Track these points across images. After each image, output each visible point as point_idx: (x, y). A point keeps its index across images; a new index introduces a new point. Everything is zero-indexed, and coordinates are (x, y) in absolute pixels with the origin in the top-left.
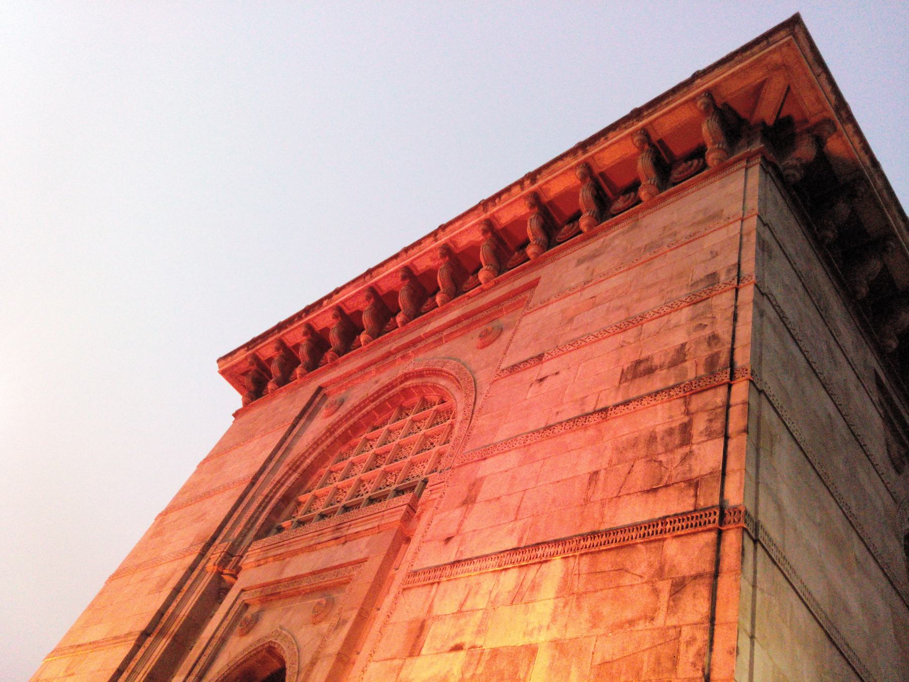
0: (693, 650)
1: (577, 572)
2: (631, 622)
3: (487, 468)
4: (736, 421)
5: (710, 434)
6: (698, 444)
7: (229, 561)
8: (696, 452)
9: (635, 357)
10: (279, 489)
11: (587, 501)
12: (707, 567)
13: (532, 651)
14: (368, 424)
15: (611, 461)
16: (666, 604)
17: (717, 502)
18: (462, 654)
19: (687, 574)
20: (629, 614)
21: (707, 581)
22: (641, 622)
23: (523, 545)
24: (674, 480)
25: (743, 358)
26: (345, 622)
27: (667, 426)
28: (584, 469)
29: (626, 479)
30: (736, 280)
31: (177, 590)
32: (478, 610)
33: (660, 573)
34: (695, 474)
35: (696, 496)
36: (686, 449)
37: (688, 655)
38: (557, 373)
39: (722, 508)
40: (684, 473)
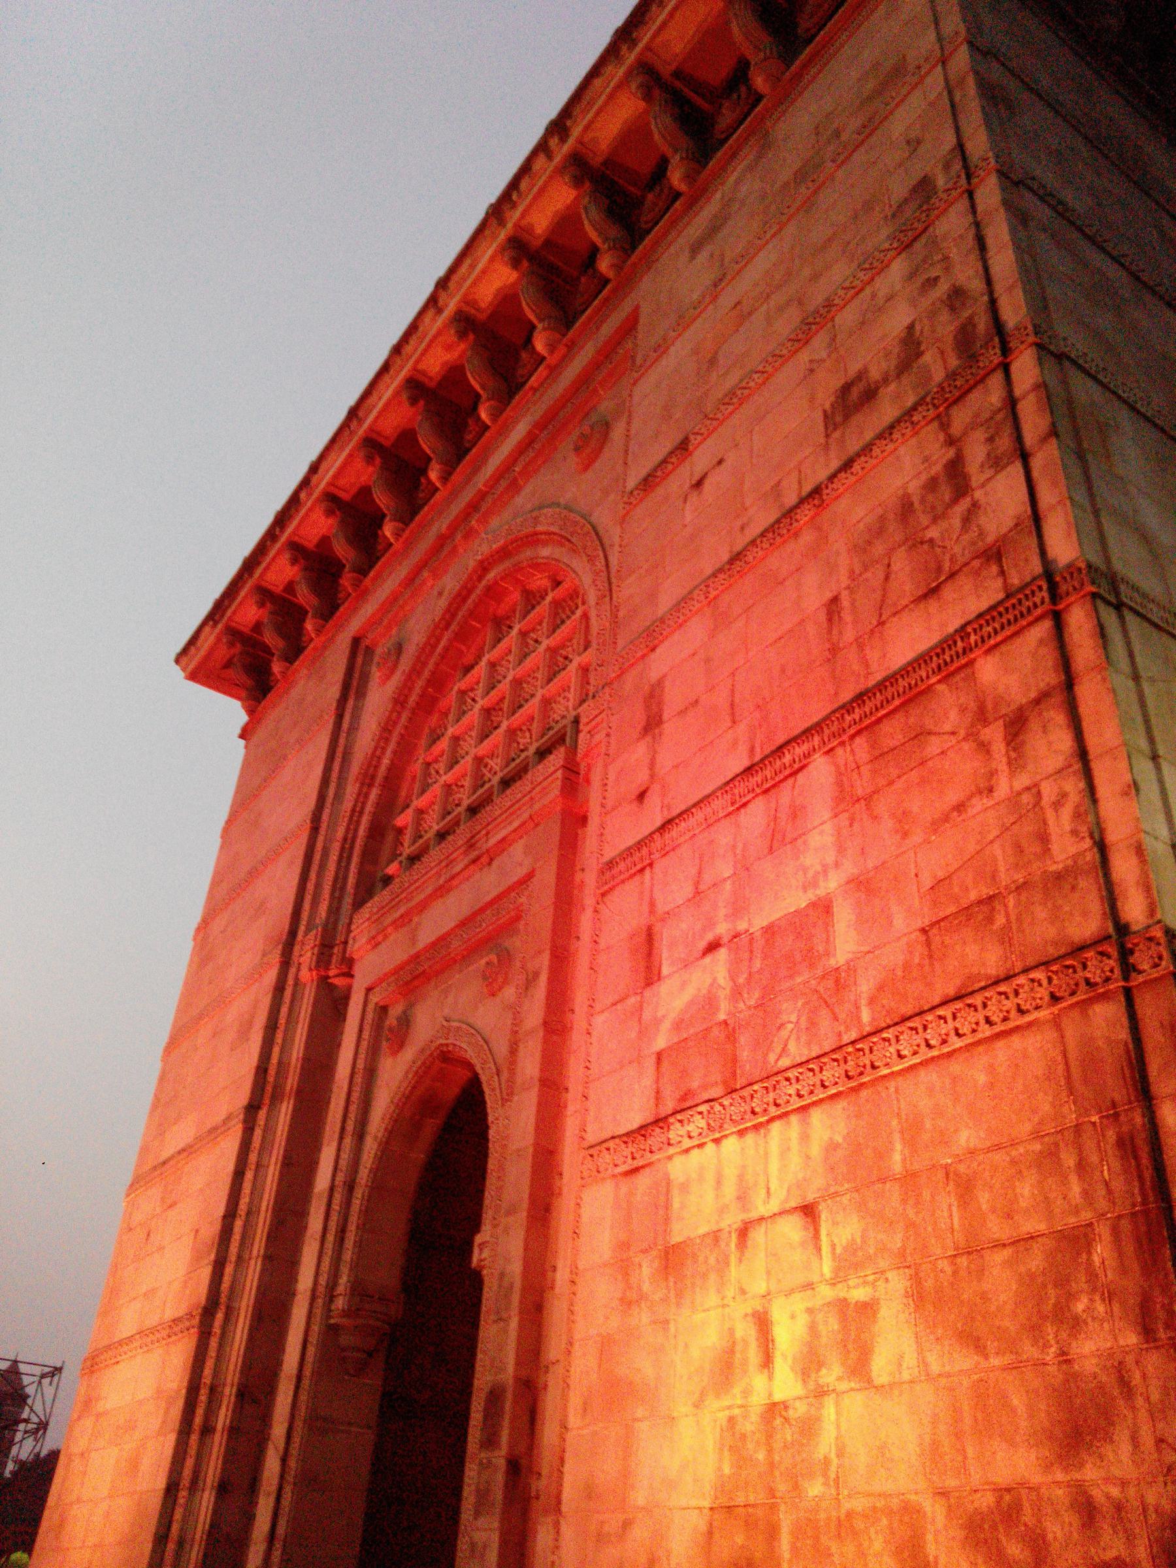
0: (1067, 812)
1: (854, 766)
2: (960, 807)
3: (660, 663)
4: (1033, 422)
5: (996, 463)
6: (983, 486)
7: (331, 956)
8: (983, 502)
9: (837, 383)
10: (358, 823)
11: (834, 650)
12: (1050, 677)
13: (824, 907)
14: (454, 668)
15: (852, 572)
16: (1004, 760)
17: (1036, 567)
18: (722, 954)
19: (1024, 701)
20: (953, 796)
21: (1057, 699)
22: (974, 801)
23: (757, 758)
24: (961, 560)
25: (1013, 311)
26: (536, 975)
27: (924, 477)
28: (814, 600)
29: (884, 589)
30: (963, 176)
31: (271, 1027)
32: (725, 880)
33: (982, 716)
34: (990, 539)
35: (1002, 573)
36: (965, 503)
37: (1061, 824)
38: (720, 462)
39: (1049, 573)
40: (974, 543)
